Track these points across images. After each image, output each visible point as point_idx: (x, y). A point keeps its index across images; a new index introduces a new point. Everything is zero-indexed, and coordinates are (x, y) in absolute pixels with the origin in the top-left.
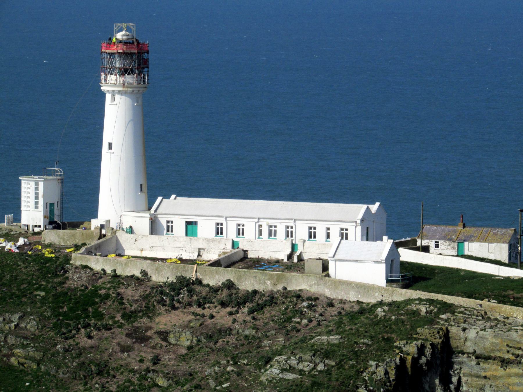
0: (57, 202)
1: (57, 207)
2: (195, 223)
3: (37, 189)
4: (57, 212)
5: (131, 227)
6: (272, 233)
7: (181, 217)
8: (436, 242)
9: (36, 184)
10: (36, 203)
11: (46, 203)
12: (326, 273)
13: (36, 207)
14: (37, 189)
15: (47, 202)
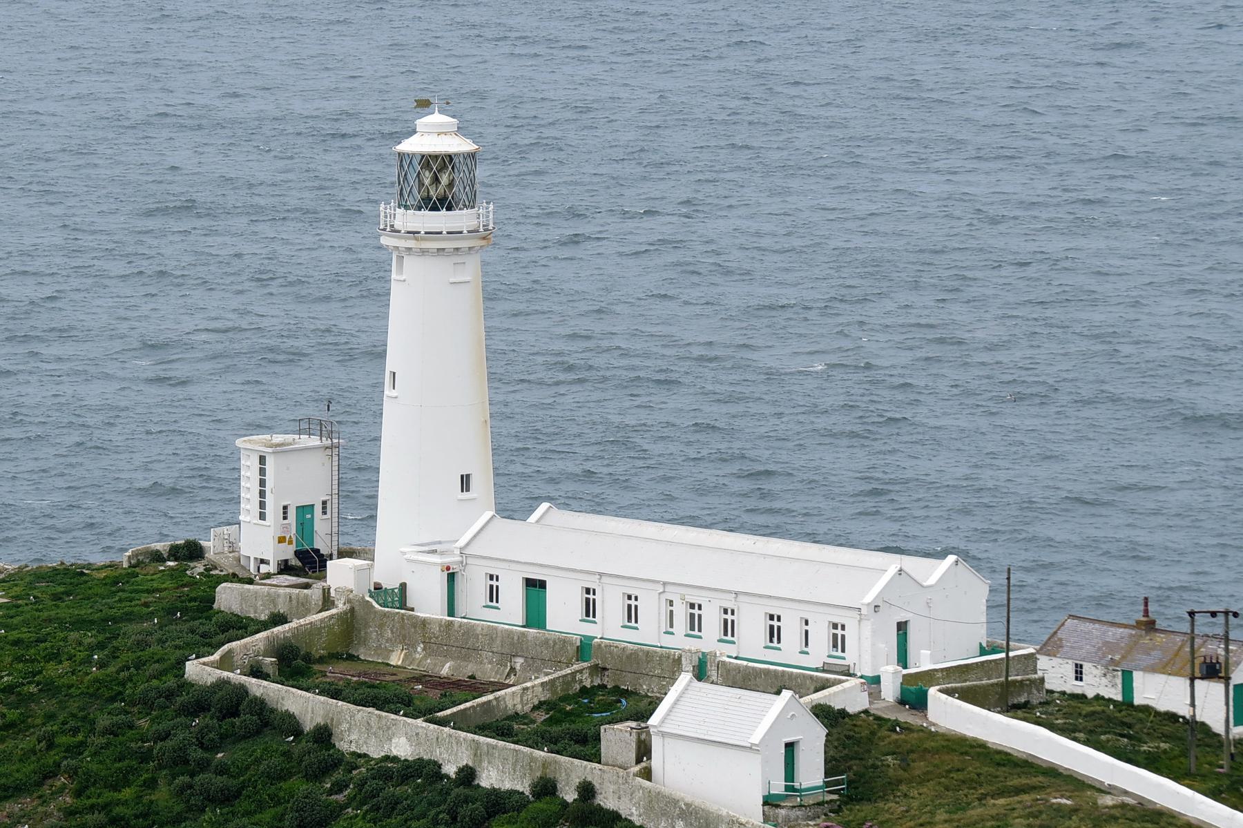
0: (324, 503)
1: (324, 513)
2: (542, 585)
3: (262, 472)
4: (321, 526)
5: (403, 586)
6: (695, 623)
7: (513, 566)
8: (1076, 665)
9: (262, 460)
10: (262, 505)
11: (285, 508)
12: (643, 765)
13: (262, 516)
14: (262, 472)
15: (286, 503)
